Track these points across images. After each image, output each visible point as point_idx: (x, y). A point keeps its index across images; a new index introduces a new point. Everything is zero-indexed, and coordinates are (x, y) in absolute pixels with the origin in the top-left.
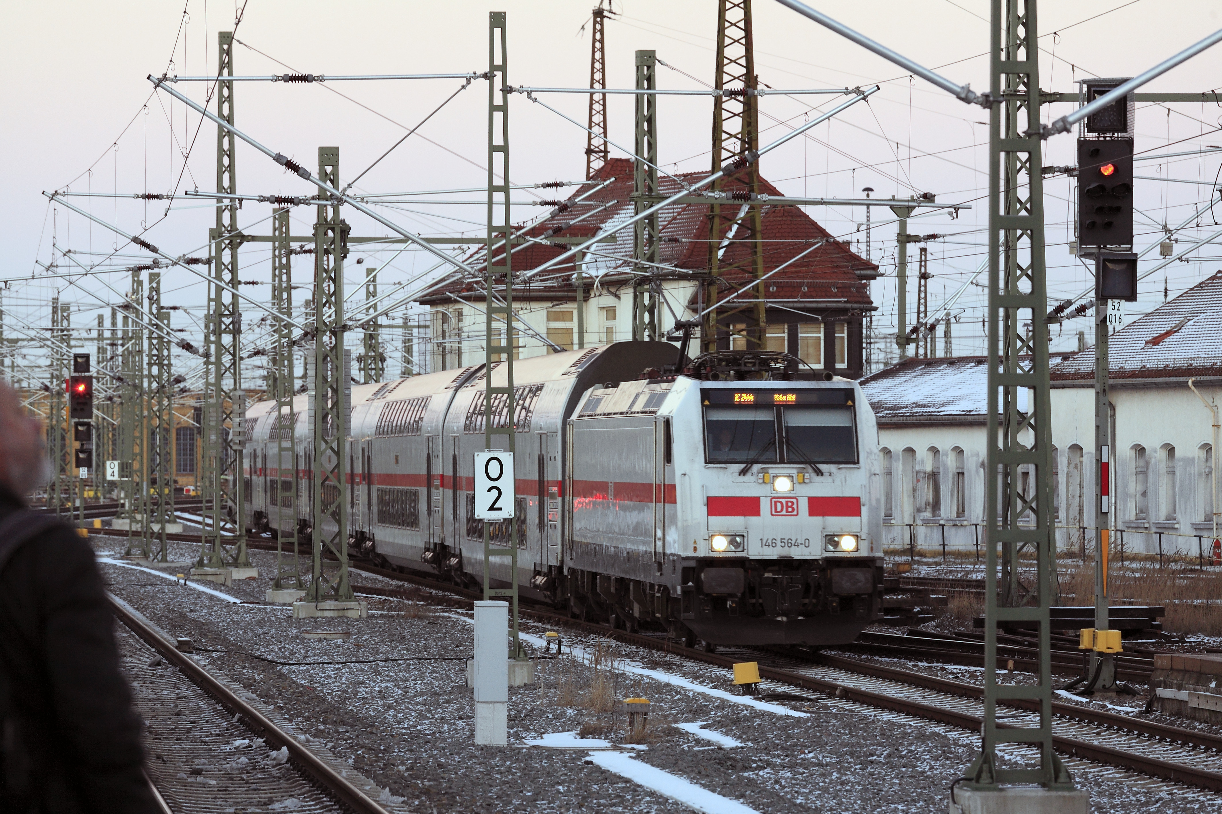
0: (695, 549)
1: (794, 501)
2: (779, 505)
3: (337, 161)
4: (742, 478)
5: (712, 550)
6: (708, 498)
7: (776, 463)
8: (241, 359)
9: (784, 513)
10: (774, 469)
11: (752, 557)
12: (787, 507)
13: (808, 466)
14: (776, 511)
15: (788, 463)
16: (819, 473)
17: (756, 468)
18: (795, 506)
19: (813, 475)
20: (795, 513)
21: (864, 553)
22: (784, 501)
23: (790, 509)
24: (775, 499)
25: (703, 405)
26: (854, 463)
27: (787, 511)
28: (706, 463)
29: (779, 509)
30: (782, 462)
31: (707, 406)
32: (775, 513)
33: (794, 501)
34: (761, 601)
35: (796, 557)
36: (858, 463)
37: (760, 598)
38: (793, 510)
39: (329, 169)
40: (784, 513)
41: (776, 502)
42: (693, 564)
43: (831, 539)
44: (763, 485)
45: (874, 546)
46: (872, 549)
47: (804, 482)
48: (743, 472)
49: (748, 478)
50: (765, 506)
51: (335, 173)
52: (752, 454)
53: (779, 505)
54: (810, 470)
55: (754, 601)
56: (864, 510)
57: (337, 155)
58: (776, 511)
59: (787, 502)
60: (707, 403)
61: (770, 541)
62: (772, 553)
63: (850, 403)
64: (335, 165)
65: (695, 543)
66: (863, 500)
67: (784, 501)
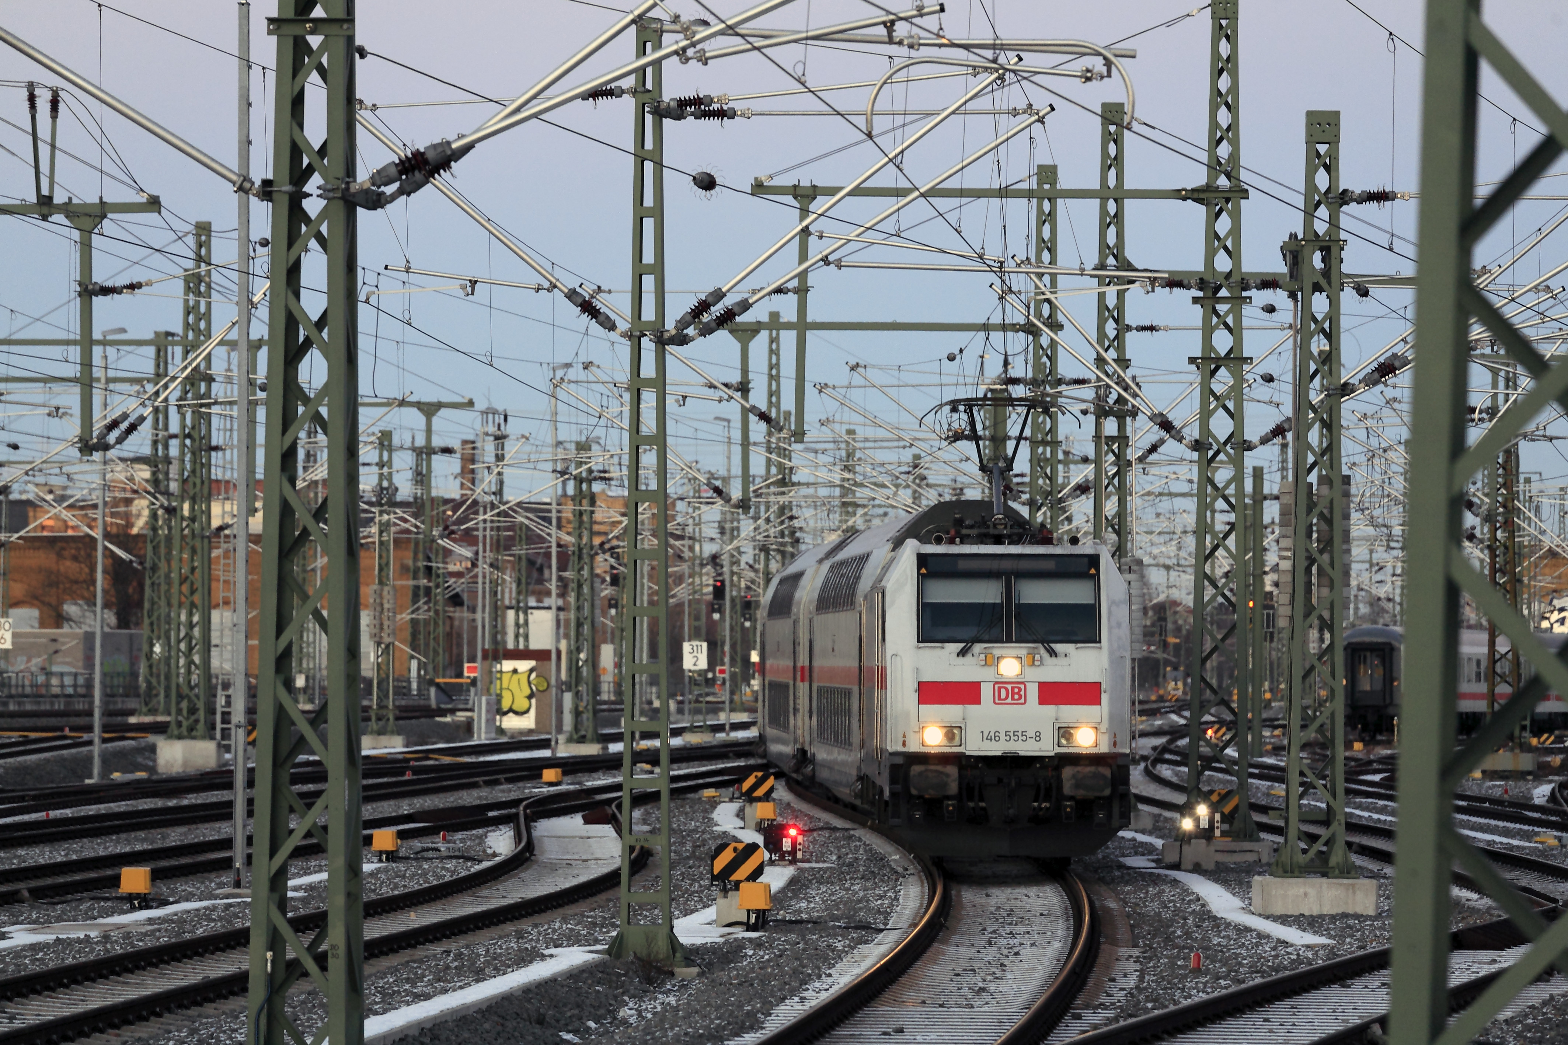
0: (904, 744)
2: (1003, 692)
3: (1337, 136)
4: (961, 660)
6: (920, 683)
7: (1002, 642)
8: (1129, 463)
9: (1009, 700)
10: (998, 649)
12: (1013, 694)
13: (1040, 645)
14: (999, 698)
15: (1016, 642)
16: (1053, 653)
17: (978, 648)
18: (1022, 693)
19: (1045, 655)
20: (1022, 701)
21: (1104, 748)
22: (1009, 687)
23: (1016, 697)
24: (999, 684)
25: (918, 573)
26: (1095, 642)
27: (1013, 699)
28: (918, 641)
29: (1003, 695)
30: (1009, 640)
31: (923, 575)
32: (998, 700)
33: (1022, 686)
34: (982, 804)
35: (1022, 754)
36: (1100, 642)
37: (982, 800)
38: (1020, 697)
39: (1322, 148)
41: (999, 689)
42: (900, 761)
43: (1065, 732)
44: (986, 668)
45: (1118, 740)
46: (1115, 744)
47: (1033, 664)
48: (962, 653)
49: (968, 658)
50: (986, 691)
51: (1334, 155)
52: (972, 632)
53: (1003, 692)
54: (1043, 651)
55: (971, 804)
56: (1105, 698)
57: (1337, 125)
58: (999, 698)
59: (1013, 688)
60: (923, 571)
61: (992, 734)
62: (995, 749)
63: (1093, 571)
64: (1334, 142)
65: (904, 736)
66: (1103, 687)
67: (1009, 687)
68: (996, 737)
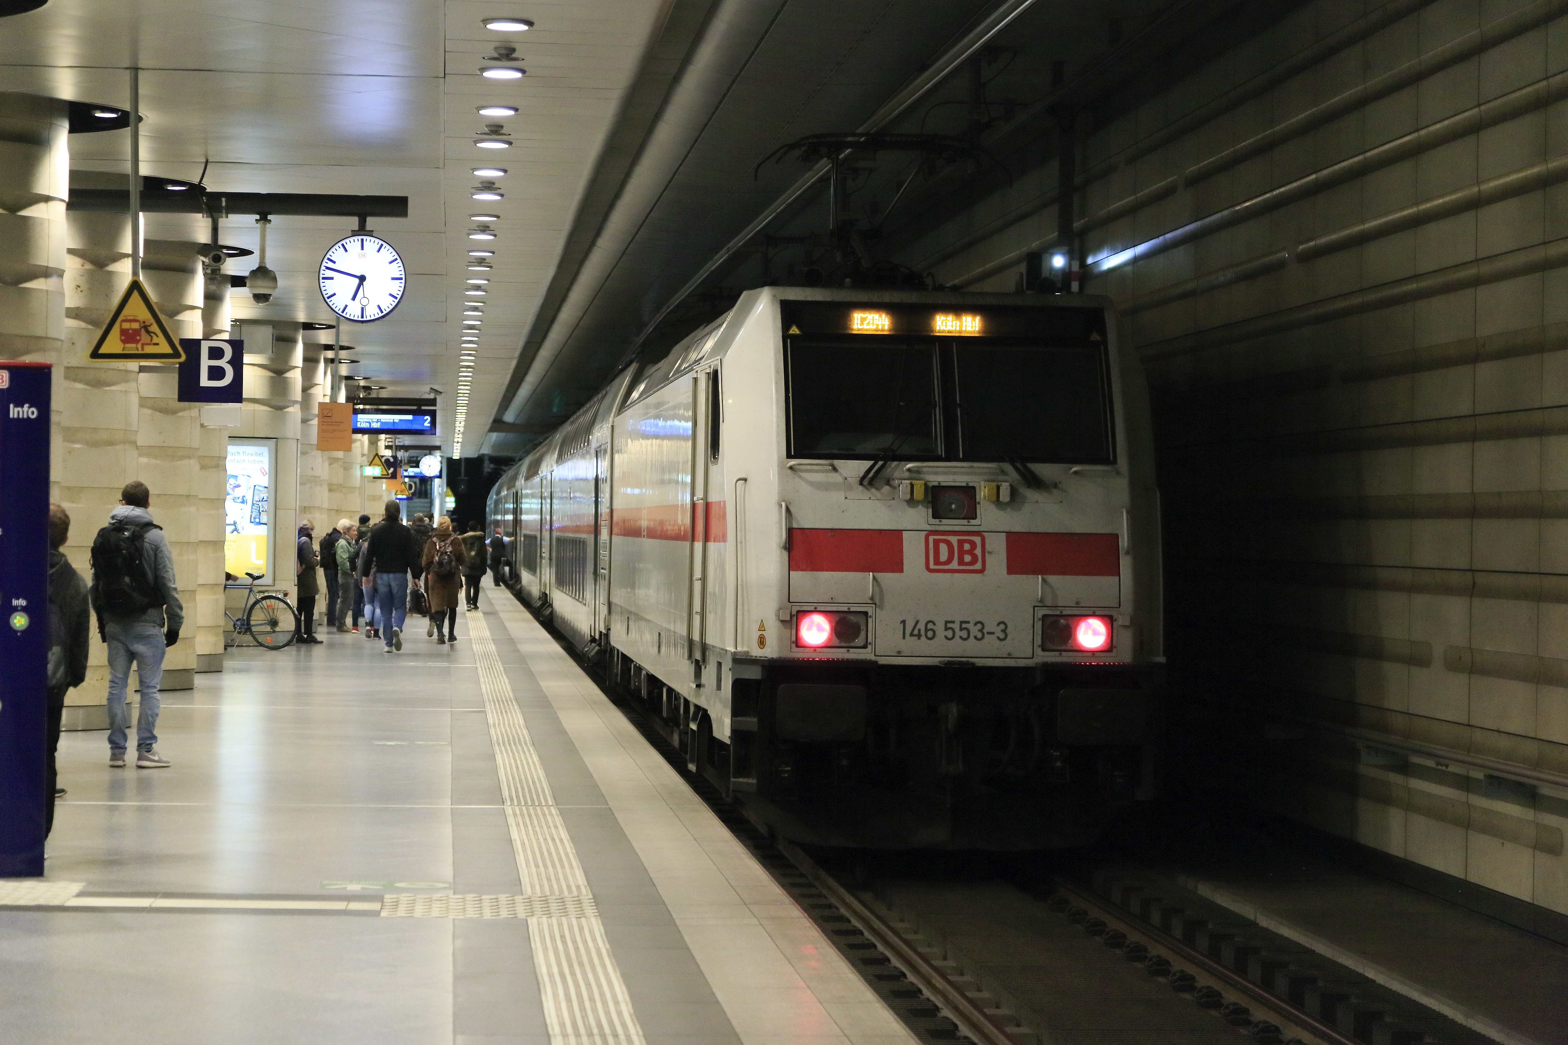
1: (977, 540)
2: (943, 548)
5: (798, 642)
7: (938, 459)
9: (954, 565)
11: (882, 661)
12: (962, 552)
14: (937, 562)
18: (978, 551)
20: (978, 566)
22: (954, 540)
27: (961, 562)
28: (789, 456)
29: (944, 556)
33: (977, 540)
38: (974, 561)
40: (954, 565)
41: (937, 543)
52: (885, 440)
53: (943, 548)
59: (961, 543)
60: (794, 330)
67: (954, 540)
68: (929, 632)
